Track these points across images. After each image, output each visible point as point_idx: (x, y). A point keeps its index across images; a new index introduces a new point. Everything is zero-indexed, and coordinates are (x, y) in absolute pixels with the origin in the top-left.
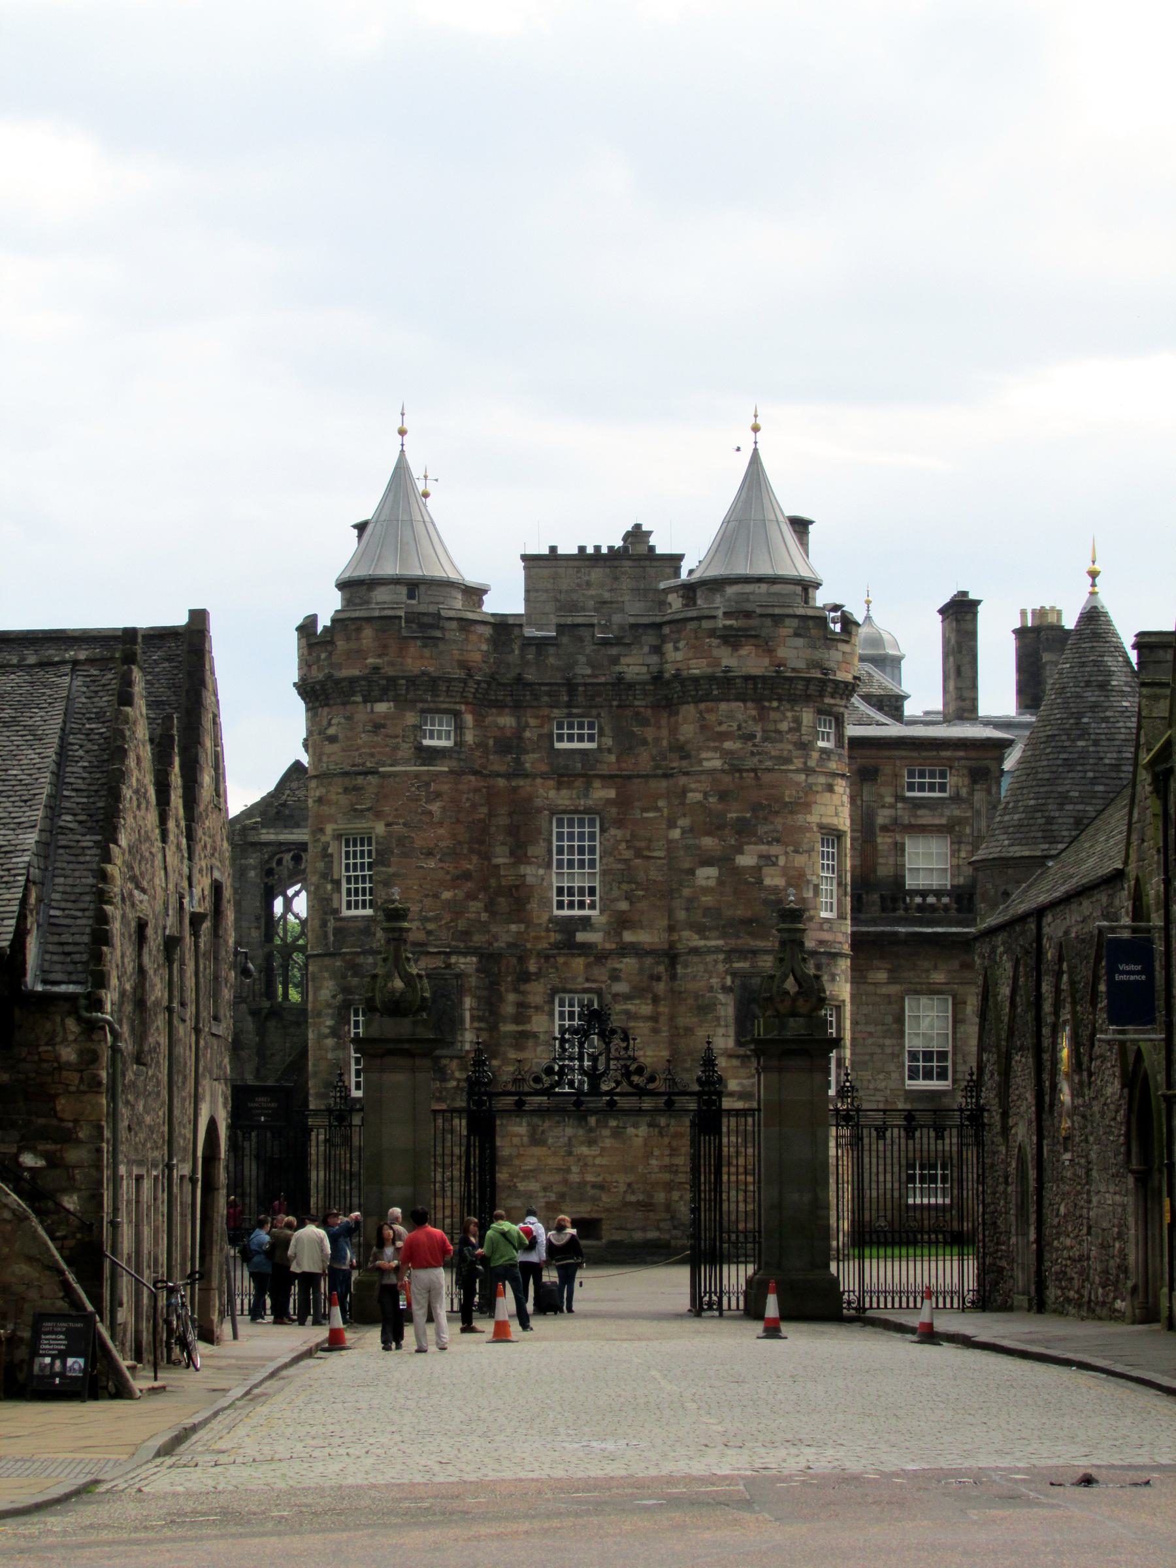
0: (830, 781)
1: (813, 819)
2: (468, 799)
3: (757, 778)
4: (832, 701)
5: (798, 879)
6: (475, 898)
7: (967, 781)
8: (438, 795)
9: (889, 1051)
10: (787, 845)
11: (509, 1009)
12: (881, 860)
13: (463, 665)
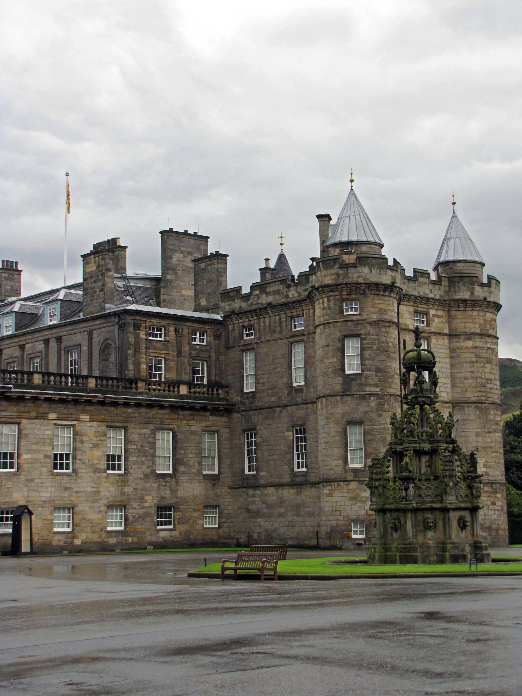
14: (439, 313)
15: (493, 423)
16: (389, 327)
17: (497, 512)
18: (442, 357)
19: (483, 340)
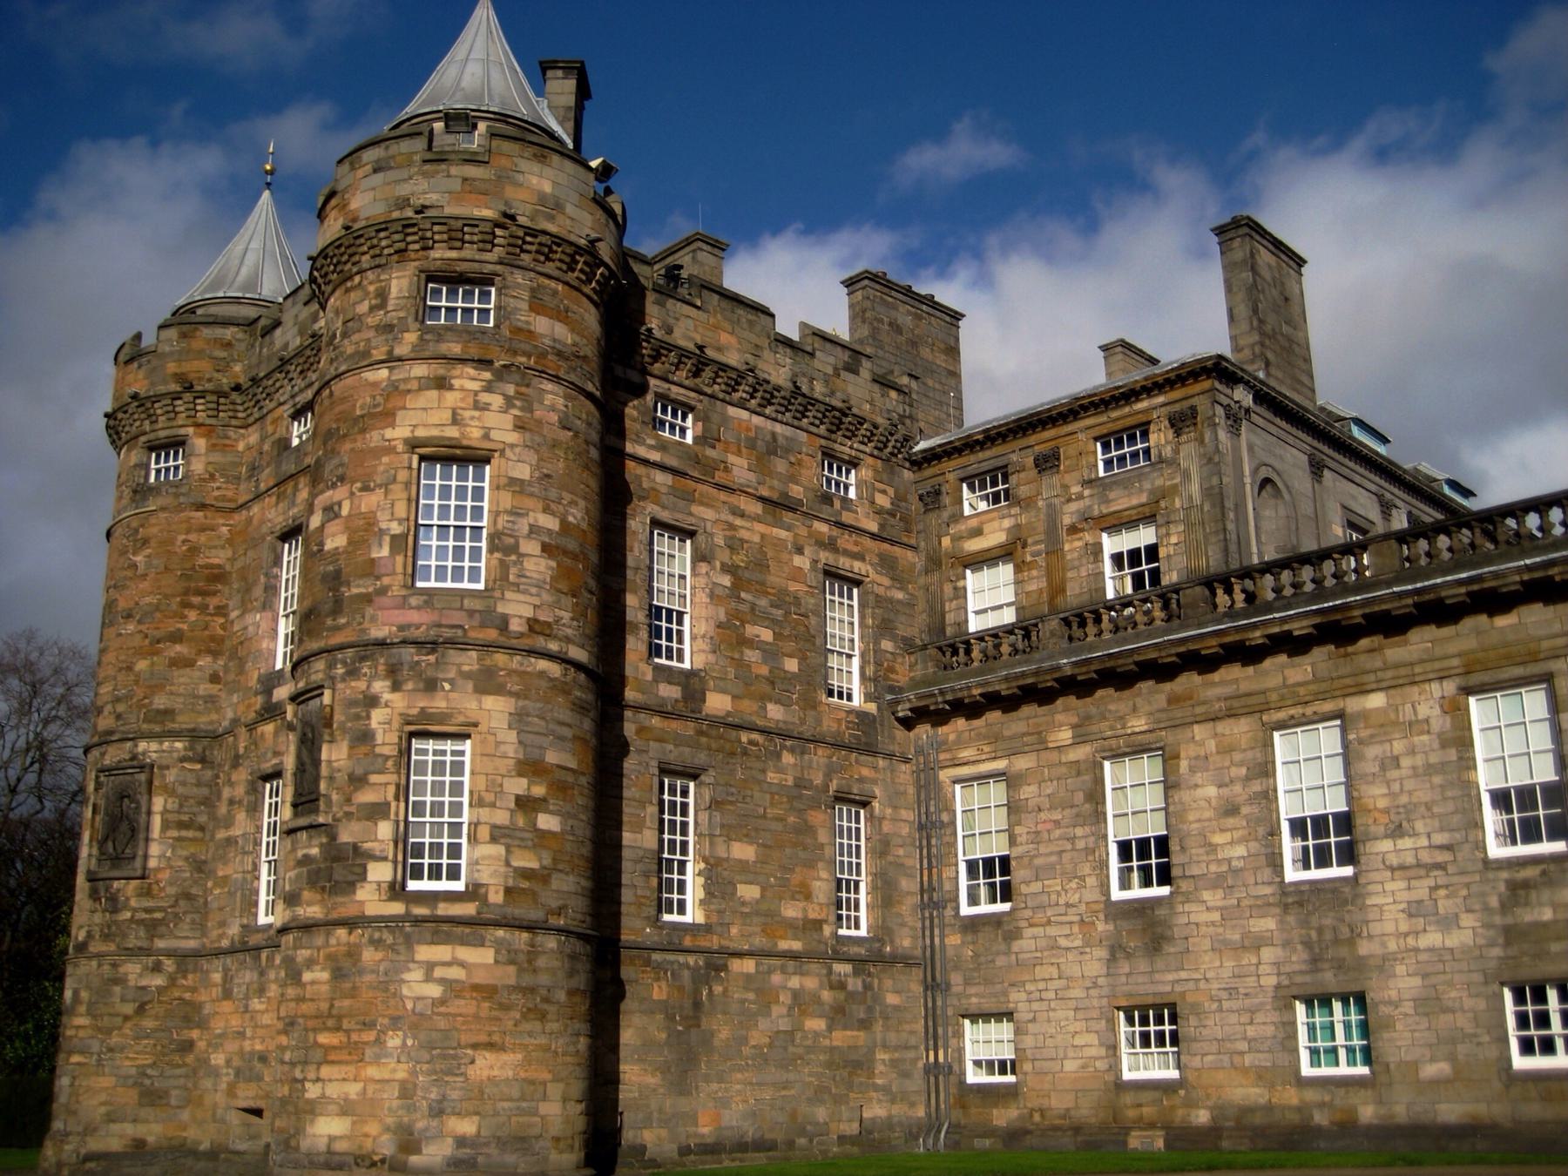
0: (441, 372)
1: (399, 433)
2: (184, 541)
3: (331, 394)
4: (454, 254)
5: (363, 531)
6: (190, 663)
7: (1170, 434)
8: (146, 542)
9: (1081, 844)
10: (353, 482)
11: (223, 809)
12: (1070, 575)
13: (179, 378)
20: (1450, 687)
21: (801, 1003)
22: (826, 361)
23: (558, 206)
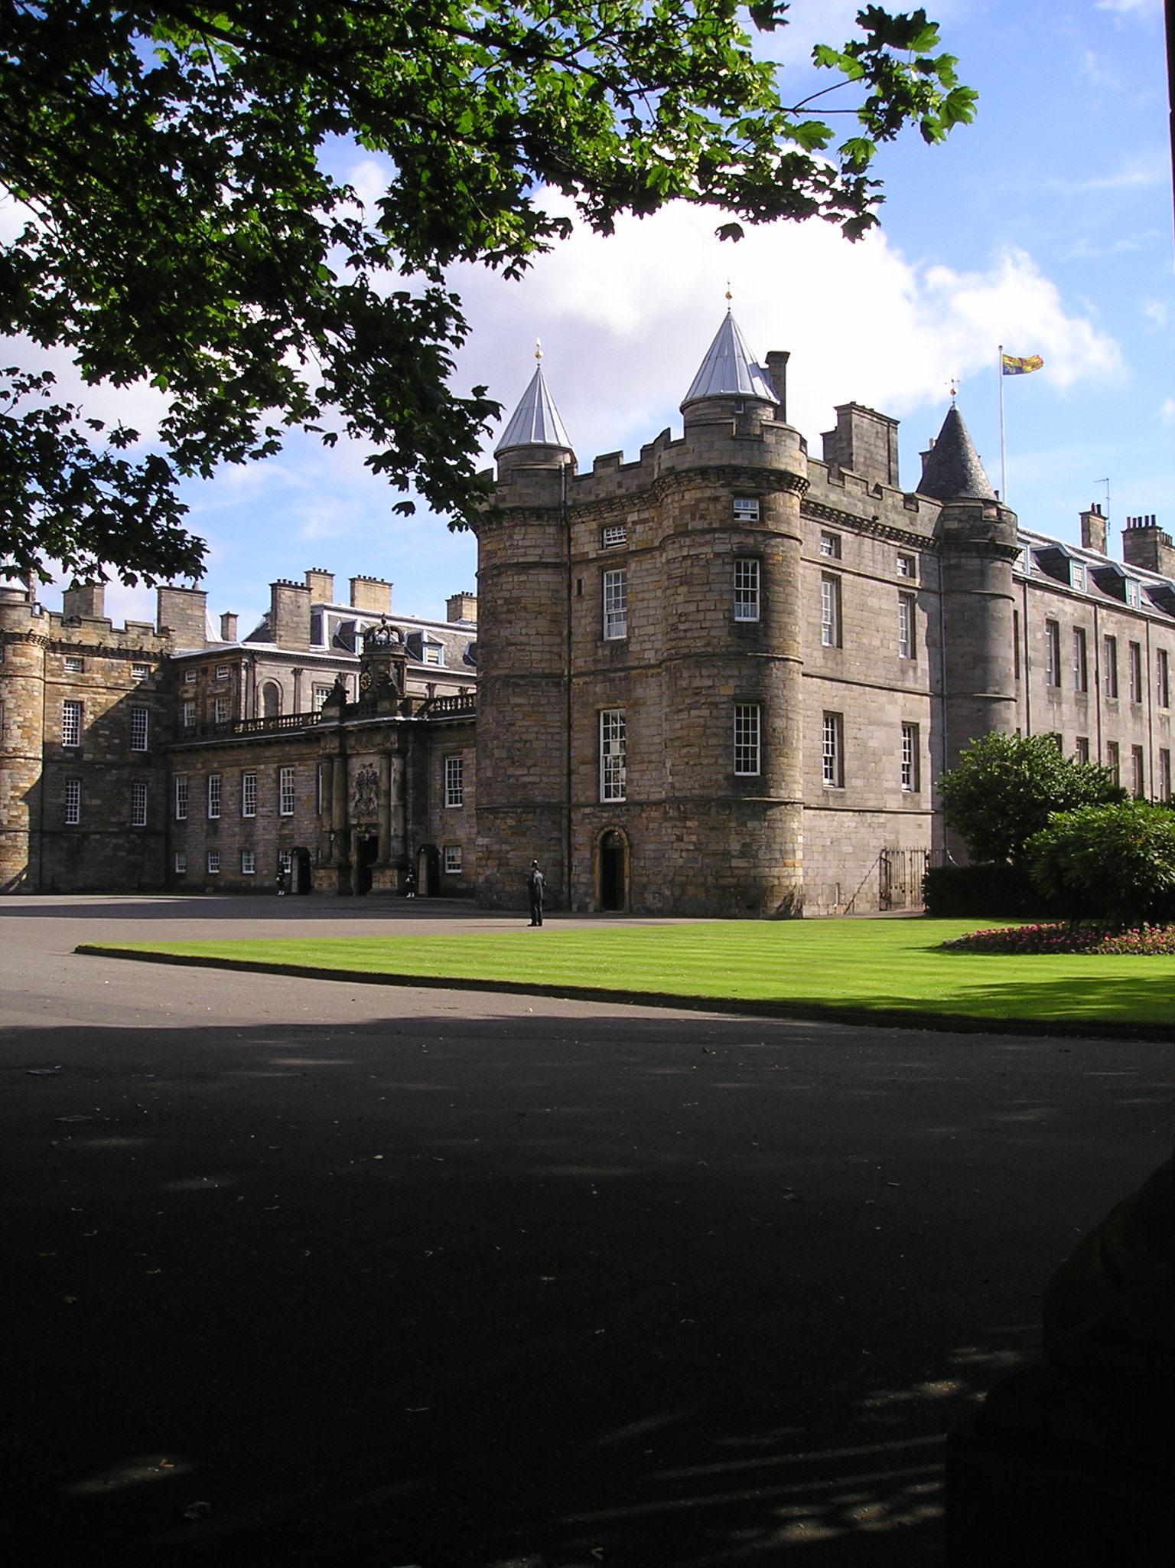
14: (646, 515)
15: (685, 693)
16: (498, 575)
17: (684, 854)
18: (648, 591)
19: (676, 546)
20: (275, 766)
21: (116, 847)
22: (133, 634)
23: (20, 623)
